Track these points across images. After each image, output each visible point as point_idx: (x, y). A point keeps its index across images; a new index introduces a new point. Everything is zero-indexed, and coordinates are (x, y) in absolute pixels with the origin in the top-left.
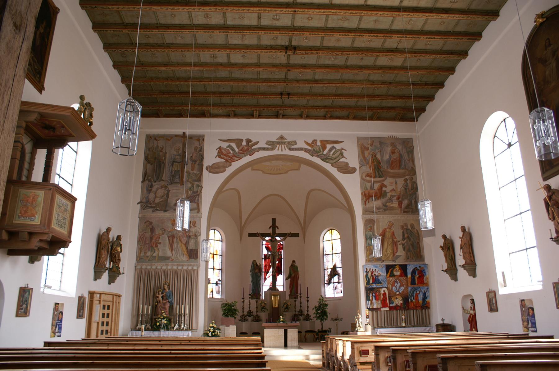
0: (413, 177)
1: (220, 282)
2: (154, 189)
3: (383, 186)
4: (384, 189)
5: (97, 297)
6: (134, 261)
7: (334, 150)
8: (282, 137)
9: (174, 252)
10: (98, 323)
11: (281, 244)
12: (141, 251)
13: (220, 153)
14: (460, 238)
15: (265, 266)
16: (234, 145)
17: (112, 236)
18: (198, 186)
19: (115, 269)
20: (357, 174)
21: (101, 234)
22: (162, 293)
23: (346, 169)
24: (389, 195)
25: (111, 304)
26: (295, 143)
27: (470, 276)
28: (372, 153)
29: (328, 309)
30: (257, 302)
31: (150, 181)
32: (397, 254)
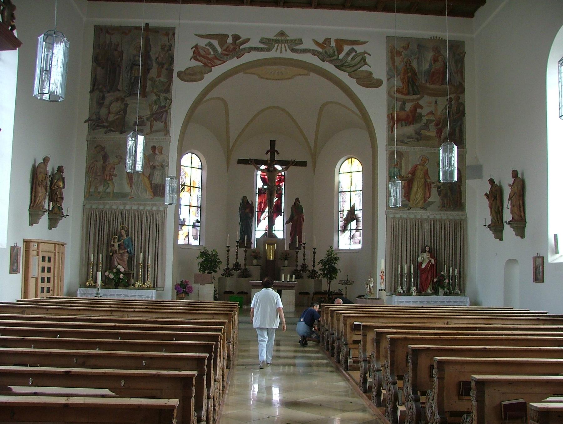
0: (461, 96)
1: (199, 224)
2: (107, 102)
3: (418, 106)
4: (419, 110)
5: (34, 247)
6: (83, 198)
7: (354, 54)
8: (282, 34)
9: (133, 187)
10: (37, 279)
11: (282, 175)
12: (90, 186)
13: (197, 53)
14: (510, 185)
15: (260, 204)
16: (215, 43)
17: (50, 168)
18: (166, 99)
19: (56, 210)
20: (383, 90)
21: (37, 165)
22: (118, 241)
23: (369, 82)
24: (424, 119)
25: (52, 256)
26: (300, 42)
27: (517, 235)
28: (405, 60)
29: (339, 265)
30: (245, 251)
31: (101, 91)
32: (429, 200)
